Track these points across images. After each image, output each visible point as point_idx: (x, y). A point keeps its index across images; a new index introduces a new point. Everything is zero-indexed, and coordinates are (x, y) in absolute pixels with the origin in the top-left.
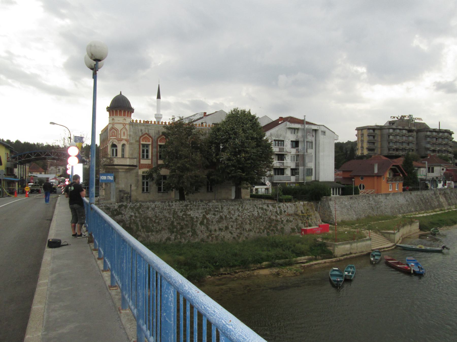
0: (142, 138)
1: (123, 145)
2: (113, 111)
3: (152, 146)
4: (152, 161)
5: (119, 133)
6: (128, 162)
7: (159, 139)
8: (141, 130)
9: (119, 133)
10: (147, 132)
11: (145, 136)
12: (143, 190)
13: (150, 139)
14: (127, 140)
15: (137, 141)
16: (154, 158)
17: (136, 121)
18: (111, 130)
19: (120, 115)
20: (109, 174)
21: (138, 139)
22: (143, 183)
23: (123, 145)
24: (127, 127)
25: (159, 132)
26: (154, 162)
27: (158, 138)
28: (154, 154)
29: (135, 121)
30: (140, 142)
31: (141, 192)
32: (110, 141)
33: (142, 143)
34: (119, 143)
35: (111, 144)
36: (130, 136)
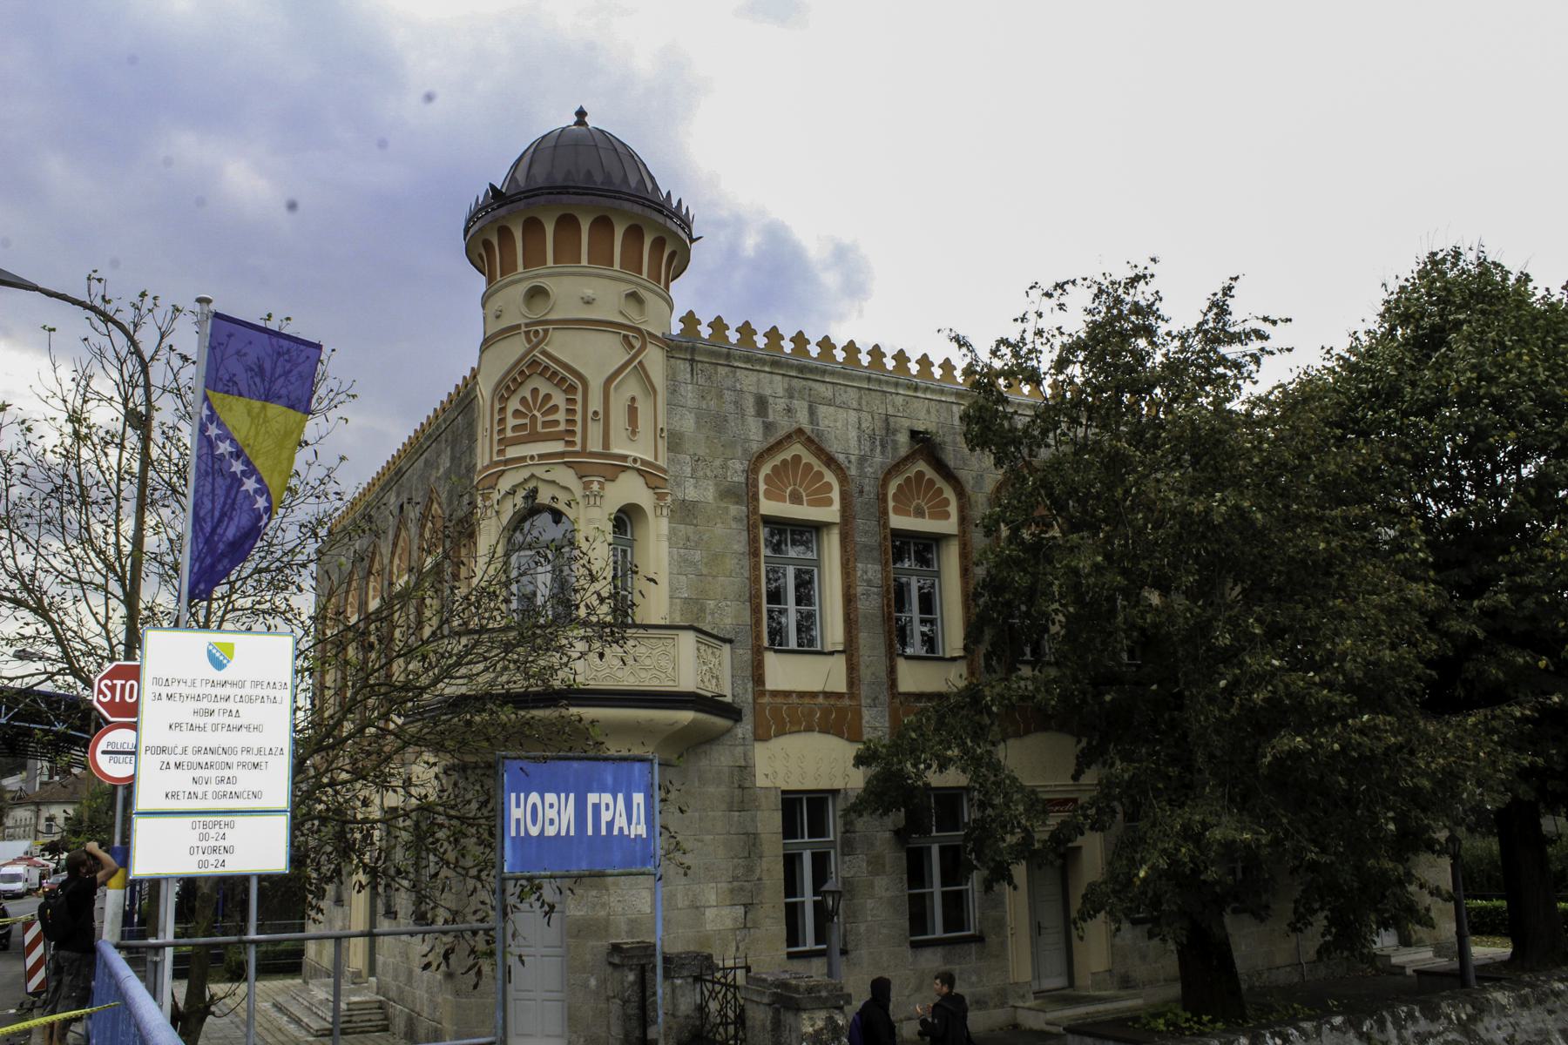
0: (766, 470)
1: (626, 519)
2: (533, 227)
3: (845, 539)
4: (852, 668)
5: (595, 404)
6: (685, 665)
7: (892, 489)
8: (762, 404)
9: (595, 404)
10: (802, 418)
11: (787, 455)
12: (793, 937)
13: (830, 477)
14: (650, 475)
15: (728, 493)
16: (863, 638)
17: (718, 325)
18: (506, 388)
19: (602, 256)
20: (608, 772)
21: (736, 472)
22: (791, 863)
23: (626, 519)
24: (654, 359)
25: (889, 430)
26: (865, 673)
27: (884, 484)
28: (870, 605)
29: (705, 332)
30: (755, 498)
31: (783, 950)
32: (505, 484)
33: (768, 507)
34: (593, 498)
36: (675, 442)
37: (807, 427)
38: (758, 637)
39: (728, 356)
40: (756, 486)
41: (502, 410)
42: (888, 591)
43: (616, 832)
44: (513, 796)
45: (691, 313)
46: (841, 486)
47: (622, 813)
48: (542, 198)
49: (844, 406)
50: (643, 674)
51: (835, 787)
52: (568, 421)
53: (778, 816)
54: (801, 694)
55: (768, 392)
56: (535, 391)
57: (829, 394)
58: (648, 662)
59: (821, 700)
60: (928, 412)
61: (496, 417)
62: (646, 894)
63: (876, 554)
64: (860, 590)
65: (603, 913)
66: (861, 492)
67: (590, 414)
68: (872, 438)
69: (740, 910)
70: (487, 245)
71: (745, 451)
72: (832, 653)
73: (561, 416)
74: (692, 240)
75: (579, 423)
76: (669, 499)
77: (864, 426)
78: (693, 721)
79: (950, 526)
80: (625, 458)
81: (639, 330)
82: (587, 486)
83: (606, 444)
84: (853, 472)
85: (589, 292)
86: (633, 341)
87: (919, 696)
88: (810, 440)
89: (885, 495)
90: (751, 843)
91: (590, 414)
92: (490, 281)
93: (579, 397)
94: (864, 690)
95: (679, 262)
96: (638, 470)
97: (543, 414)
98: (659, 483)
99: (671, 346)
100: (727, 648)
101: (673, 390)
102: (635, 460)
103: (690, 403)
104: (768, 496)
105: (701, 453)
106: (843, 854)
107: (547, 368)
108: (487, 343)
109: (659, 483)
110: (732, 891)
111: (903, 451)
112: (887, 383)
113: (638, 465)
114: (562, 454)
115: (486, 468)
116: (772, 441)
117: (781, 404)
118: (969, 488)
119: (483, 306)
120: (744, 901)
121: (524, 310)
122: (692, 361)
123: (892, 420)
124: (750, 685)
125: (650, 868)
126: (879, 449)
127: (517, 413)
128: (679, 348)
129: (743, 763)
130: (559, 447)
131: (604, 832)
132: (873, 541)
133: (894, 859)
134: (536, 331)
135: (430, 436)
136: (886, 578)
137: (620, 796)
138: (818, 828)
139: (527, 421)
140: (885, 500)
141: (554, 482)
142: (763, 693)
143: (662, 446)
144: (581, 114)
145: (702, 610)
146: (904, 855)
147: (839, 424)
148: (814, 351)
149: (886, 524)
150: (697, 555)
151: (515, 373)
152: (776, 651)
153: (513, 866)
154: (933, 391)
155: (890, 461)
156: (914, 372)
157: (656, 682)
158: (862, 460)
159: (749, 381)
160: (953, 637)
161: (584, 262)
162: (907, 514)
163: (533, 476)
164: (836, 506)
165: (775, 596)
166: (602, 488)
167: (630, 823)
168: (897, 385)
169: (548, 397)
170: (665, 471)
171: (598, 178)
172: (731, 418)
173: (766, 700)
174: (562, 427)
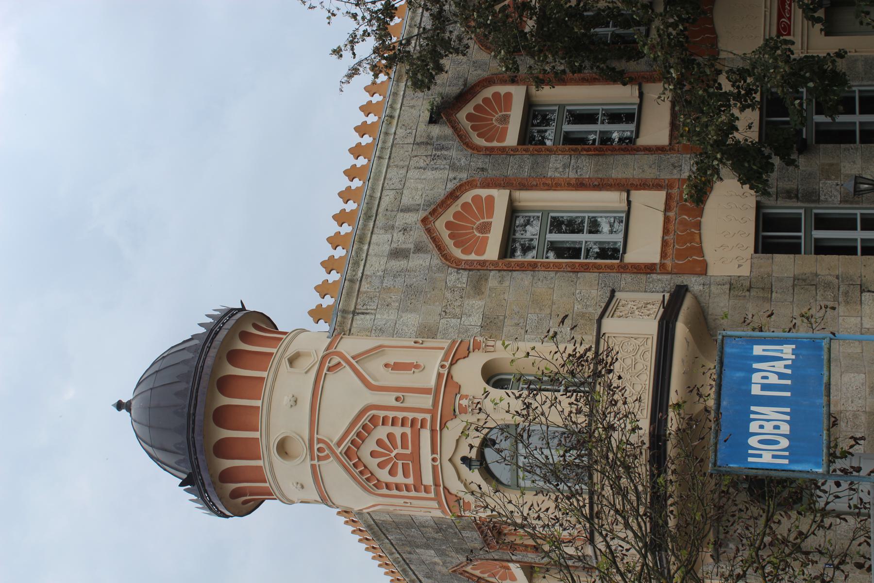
0: (457, 253)
2: (223, 449)
3: (525, 186)
5: (389, 399)
6: (633, 330)
7: (482, 142)
8: (397, 254)
10: (413, 218)
11: (445, 234)
13: (467, 197)
15: (477, 288)
16: (617, 173)
18: (366, 479)
19: (254, 386)
21: (459, 279)
25: (428, 142)
26: (650, 174)
27: (476, 149)
28: (586, 167)
30: (483, 263)
32: (456, 487)
33: (492, 252)
35: (475, 476)
36: (428, 332)
37: (422, 214)
38: (611, 267)
39: (352, 281)
40: (472, 261)
41: (388, 486)
42: (575, 150)
43: (789, 371)
44: (750, 459)
45: (311, 313)
46: (476, 187)
47: (772, 366)
48: (198, 438)
49: (404, 181)
50: (639, 367)
51: (754, 205)
52: (403, 425)
53: (781, 259)
54: (666, 231)
55: (387, 248)
56: (373, 454)
57: (392, 194)
58: (628, 362)
59: (671, 214)
60: (413, 107)
61: (395, 492)
62: (846, 378)
63: (540, 159)
64: (572, 175)
65: (863, 418)
66: (483, 169)
67: (398, 404)
68: (434, 158)
69: (866, 296)
70: (236, 494)
71: (439, 270)
72: (629, 203)
73: (398, 431)
74: (243, 309)
75: (405, 414)
76: (479, 339)
77: (422, 164)
78: (686, 324)
79: (518, 93)
80: (439, 376)
81: (324, 358)
82: (463, 410)
83: (425, 391)
84: (464, 176)
85: (286, 400)
86: (333, 363)
87: (674, 126)
88: (433, 213)
89: (487, 148)
90: (802, 283)
91: (398, 404)
92: (268, 494)
93: (382, 414)
94: (665, 175)
95: (263, 321)
96: (452, 364)
97: (395, 447)
98: (464, 347)
99: (340, 331)
100: (618, 295)
101: (382, 331)
102: (443, 366)
103: (393, 317)
104: (481, 251)
105: (439, 309)
106: (818, 201)
107: (353, 442)
108: (325, 499)
109: (464, 347)
110: (847, 303)
111: (448, 131)
112: (384, 142)
113: (447, 364)
114: (433, 431)
115: (440, 504)
116: (431, 246)
117: (398, 236)
118: (485, 75)
119: (291, 502)
120: (858, 293)
121: (297, 461)
122: (354, 313)
123: (418, 140)
124: (654, 276)
125: (825, 344)
126: (445, 152)
127: (392, 473)
128: (342, 324)
129: (727, 286)
130: (426, 435)
131: (789, 382)
132: (528, 161)
133: (825, 155)
134: (318, 450)
135: (404, 571)
136: (563, 152)
137: (756, 366)
138: (793, 223)
139: (400, 463)
140: (491, 149)
141: (458, 441)
142: (663, 265)
143: (430, 343)
144: (120, 406)
145: (583, 315)
146: (821, 146)
147: (420, 186)
148: (351, 206)
149: (514, 150)
150: (532, 317)
151: (355, 472)
152: (624, 252)
153: (818, 465)
154: (394, 102)
155: (456, 143)
156: (375, 119)
157: (648, 355)
158: (453, 167)
159: (376, 264)
160: (620, 95)
161: (258, 403)
162: (504, 132)
163: (450, 460)
164: (494, 192)
165: (574, 252)
166: (466, 397)
167: (780, 359)
168: (386, 134)
169: (379, 442)
170: (454, 342)
171: (182, 386)
172: (408, 282)
173: (668, 262)
174: (408, 430)
